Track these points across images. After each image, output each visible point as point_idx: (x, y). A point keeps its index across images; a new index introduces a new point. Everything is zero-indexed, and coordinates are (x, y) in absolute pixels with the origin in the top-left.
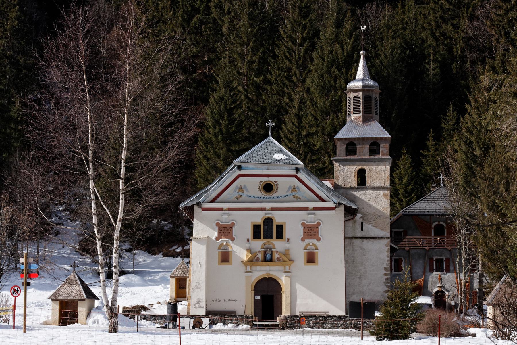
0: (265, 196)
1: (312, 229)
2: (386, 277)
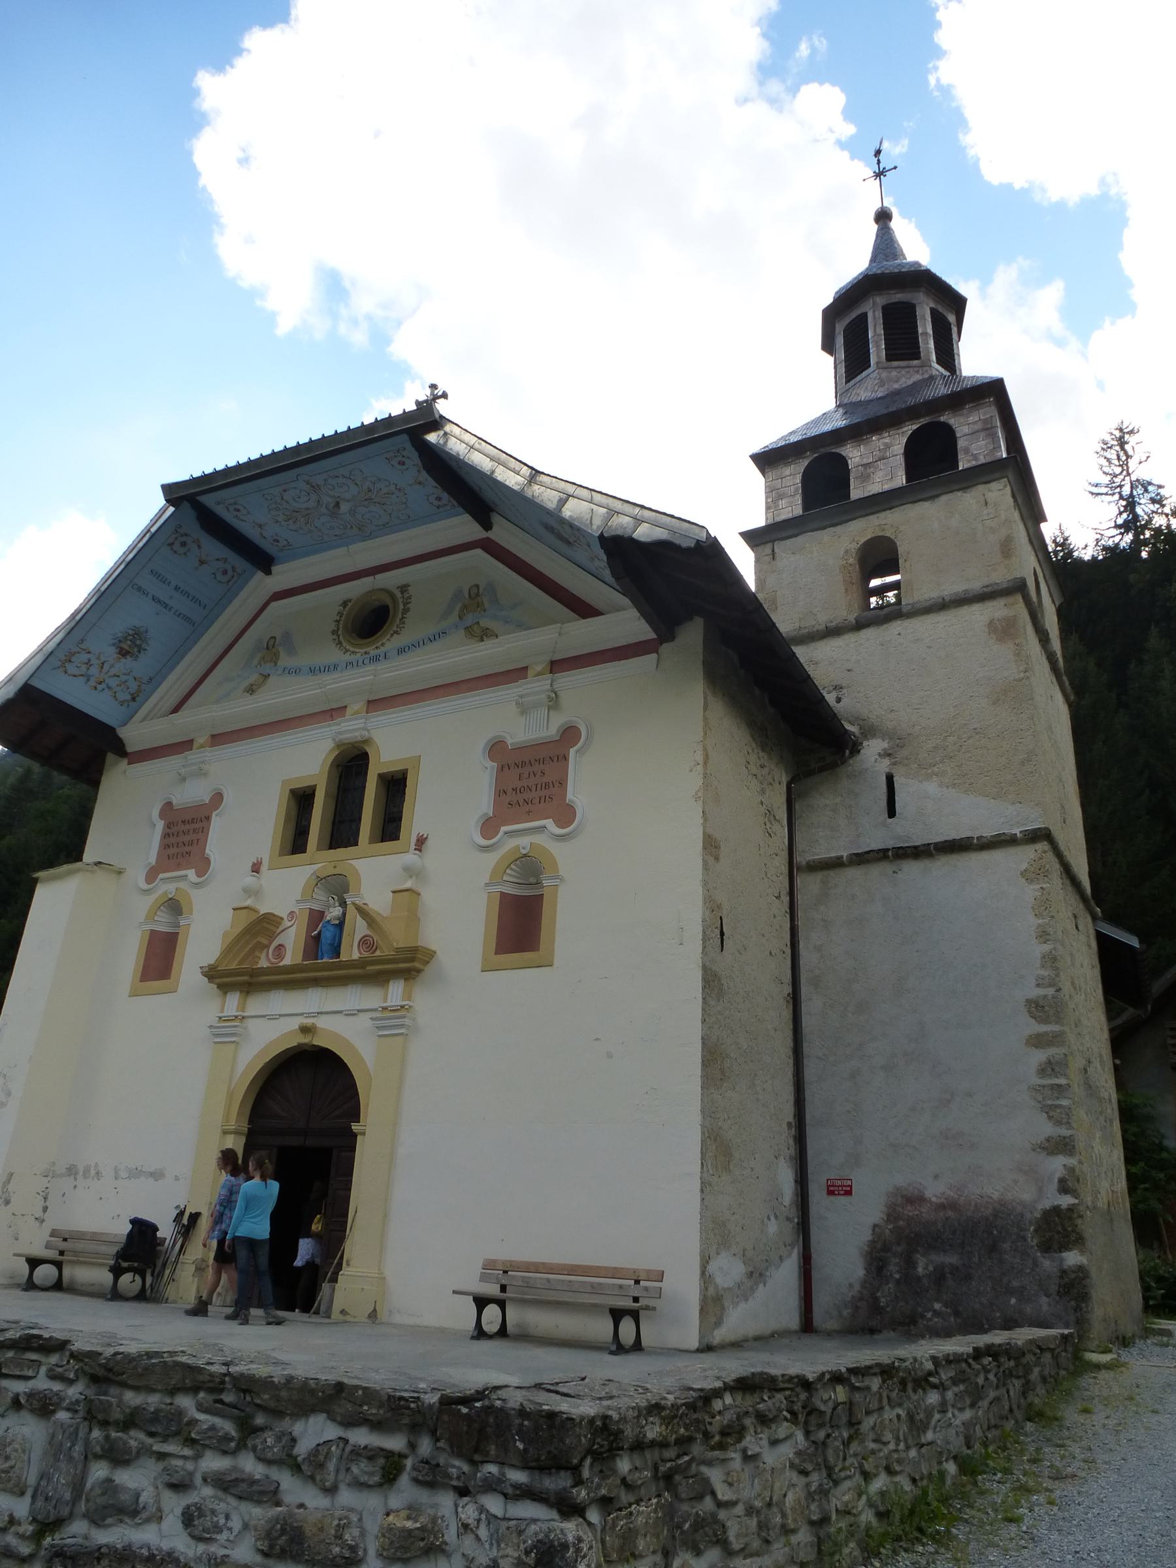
0: (353, 658)
2: (1039, 1056)
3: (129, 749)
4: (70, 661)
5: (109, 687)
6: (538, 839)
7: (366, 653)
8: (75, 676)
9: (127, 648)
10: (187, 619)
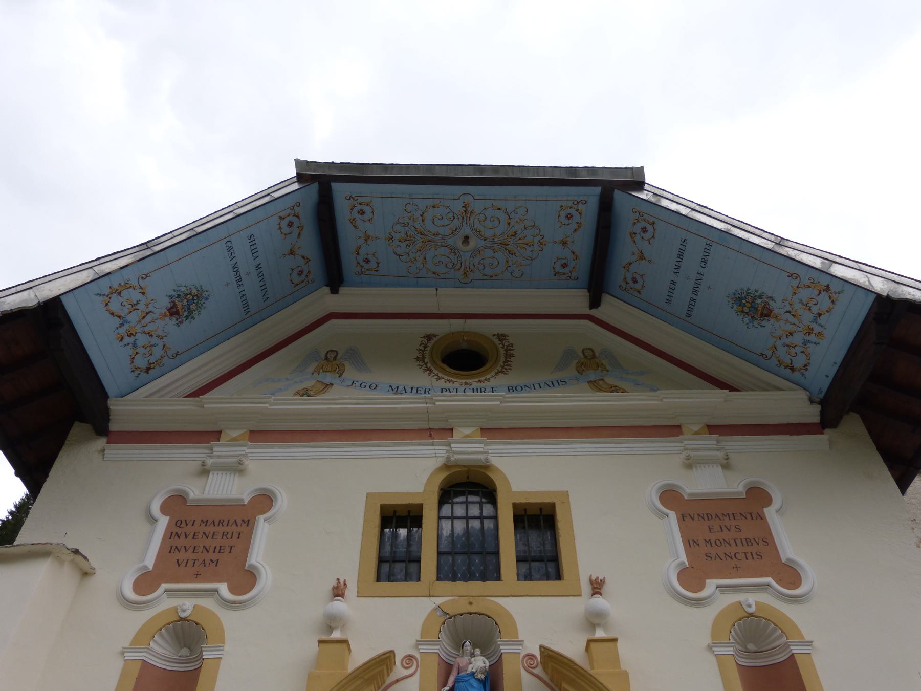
0: (448, 385)
1: (727, 522)
3: (113, 427)
4: (119, 293)
5: (135, 345)
6: (765, 598)
7: (466, 384)
8: (112, 314)
9: (179, 307)
10: (246, 305)
